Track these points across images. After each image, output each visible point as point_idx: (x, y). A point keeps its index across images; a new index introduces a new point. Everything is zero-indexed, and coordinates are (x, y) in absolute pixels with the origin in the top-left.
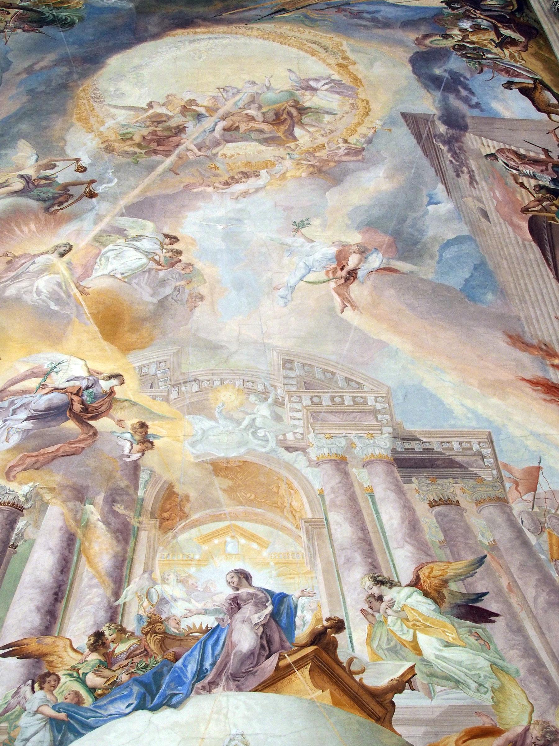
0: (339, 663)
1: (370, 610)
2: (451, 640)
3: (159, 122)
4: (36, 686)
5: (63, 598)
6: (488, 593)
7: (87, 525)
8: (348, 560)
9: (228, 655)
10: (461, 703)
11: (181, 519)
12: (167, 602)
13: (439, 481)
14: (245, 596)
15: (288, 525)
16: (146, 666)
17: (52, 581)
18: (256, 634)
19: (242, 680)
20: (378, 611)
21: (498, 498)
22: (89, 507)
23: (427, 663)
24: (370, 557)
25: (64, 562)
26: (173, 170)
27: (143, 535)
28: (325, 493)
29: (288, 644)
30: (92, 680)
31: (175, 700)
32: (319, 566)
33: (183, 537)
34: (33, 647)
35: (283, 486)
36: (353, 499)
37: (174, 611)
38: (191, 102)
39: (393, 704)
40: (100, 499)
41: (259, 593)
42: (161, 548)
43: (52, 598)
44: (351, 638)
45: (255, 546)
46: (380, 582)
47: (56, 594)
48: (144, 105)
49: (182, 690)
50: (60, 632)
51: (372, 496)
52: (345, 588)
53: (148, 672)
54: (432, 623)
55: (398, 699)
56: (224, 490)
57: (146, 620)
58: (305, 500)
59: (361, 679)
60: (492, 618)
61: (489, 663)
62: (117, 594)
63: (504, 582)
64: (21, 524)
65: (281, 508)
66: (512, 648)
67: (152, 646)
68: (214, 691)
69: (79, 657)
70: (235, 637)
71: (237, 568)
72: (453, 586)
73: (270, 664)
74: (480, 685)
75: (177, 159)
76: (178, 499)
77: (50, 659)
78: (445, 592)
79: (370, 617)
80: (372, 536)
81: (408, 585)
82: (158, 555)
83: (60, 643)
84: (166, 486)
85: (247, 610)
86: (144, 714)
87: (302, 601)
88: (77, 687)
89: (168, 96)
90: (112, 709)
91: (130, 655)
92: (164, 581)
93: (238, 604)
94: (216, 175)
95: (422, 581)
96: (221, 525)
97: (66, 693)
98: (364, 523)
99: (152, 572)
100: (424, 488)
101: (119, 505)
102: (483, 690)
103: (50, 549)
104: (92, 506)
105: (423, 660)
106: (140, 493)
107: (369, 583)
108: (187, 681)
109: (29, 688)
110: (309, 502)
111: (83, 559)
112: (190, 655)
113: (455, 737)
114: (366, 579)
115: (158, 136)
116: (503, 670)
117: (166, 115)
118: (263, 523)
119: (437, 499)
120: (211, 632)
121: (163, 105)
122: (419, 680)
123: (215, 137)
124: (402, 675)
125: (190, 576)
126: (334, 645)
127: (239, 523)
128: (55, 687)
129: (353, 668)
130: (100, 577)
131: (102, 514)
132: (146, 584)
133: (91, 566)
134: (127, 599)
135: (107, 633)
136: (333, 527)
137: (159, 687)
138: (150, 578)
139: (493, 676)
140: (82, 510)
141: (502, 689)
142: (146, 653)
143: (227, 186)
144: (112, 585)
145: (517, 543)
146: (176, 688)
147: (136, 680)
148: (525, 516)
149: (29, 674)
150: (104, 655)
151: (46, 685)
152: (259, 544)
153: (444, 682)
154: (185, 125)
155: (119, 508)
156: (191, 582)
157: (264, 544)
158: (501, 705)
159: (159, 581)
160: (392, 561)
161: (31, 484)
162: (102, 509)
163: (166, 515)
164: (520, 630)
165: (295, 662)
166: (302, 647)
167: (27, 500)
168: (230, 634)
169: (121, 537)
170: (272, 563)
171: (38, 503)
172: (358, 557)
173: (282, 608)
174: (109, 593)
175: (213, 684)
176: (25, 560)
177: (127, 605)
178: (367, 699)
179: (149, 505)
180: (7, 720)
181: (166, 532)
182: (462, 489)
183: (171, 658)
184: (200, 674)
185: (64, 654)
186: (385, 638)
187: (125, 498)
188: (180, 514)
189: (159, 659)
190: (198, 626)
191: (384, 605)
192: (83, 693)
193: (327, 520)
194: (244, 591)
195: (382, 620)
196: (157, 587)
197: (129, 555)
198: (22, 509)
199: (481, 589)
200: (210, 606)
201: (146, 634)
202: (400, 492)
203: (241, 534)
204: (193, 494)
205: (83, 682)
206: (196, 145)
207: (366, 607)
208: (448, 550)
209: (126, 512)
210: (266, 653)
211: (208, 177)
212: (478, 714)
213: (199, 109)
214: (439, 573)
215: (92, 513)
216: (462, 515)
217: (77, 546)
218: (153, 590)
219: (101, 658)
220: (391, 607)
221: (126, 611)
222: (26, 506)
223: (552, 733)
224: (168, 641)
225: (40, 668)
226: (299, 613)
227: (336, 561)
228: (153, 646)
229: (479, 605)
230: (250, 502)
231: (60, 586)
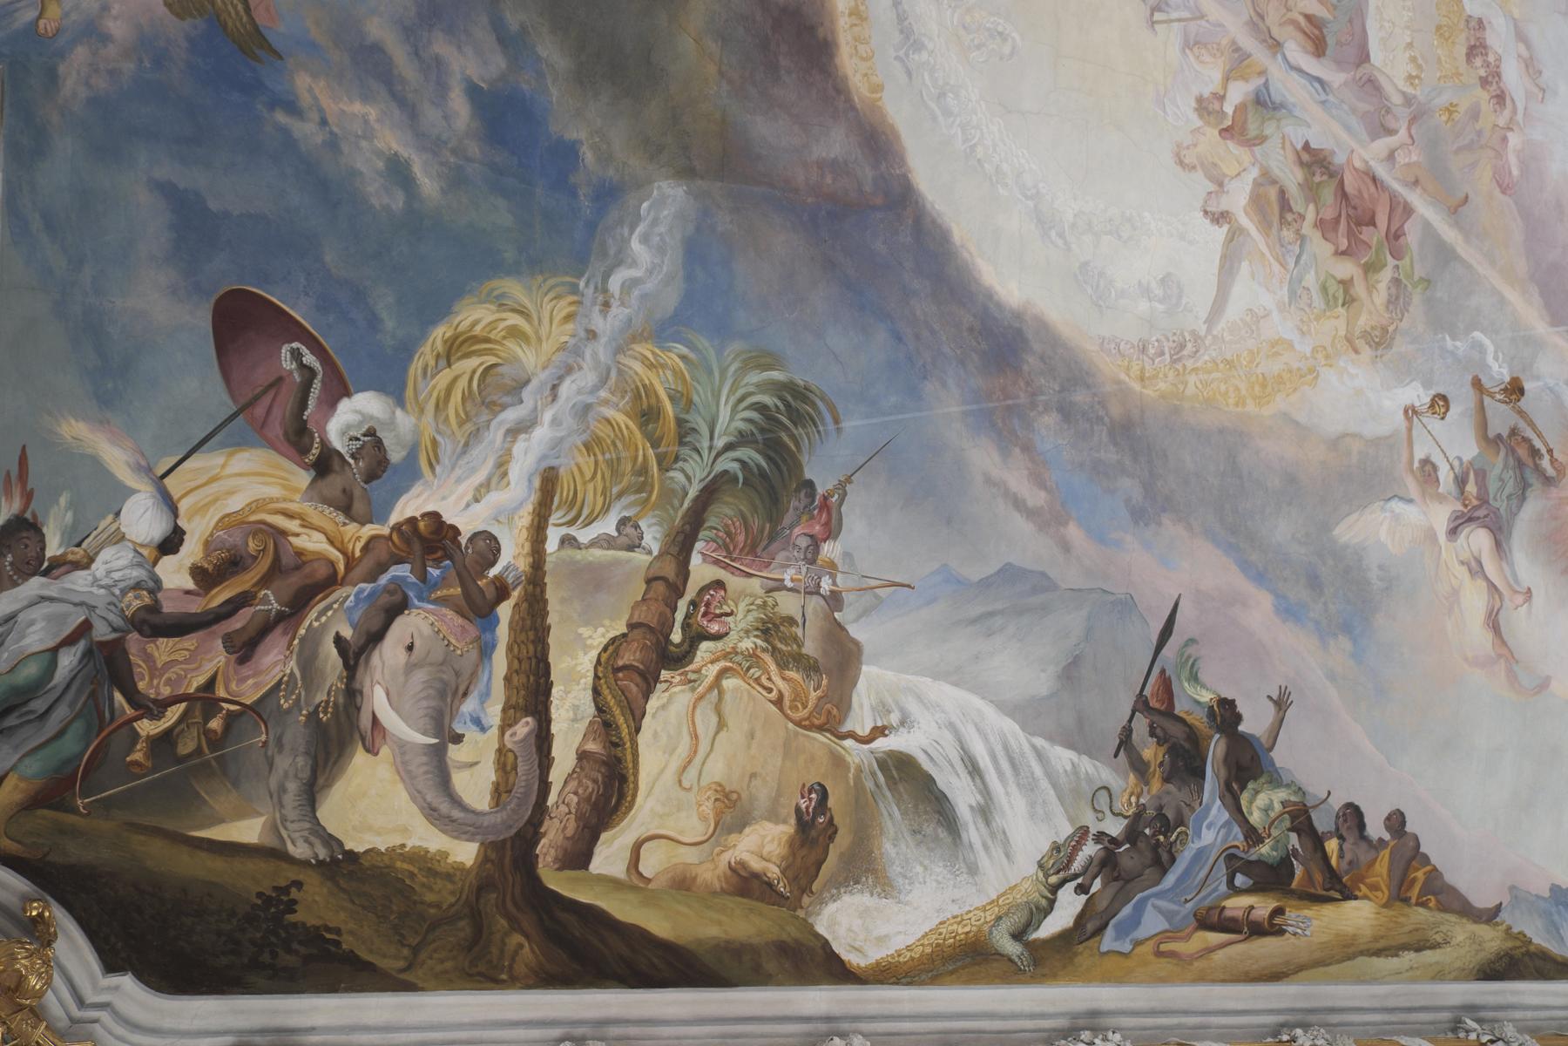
3: (1285, 204)
26: (1457, 208)
38: (1206, 107)
48: (1221, 232)
75: (1419, 190)
89: (1181, 163)
94: (1475, 114)
115: (1337, 220)
117: (1257, 184)
121: (1221, 185)
123: (1345, 84)
143: (1508, 101)
154: (1299, 146)
206: (1374, 136)
211: (1479, 133)
213: (1238, 93)
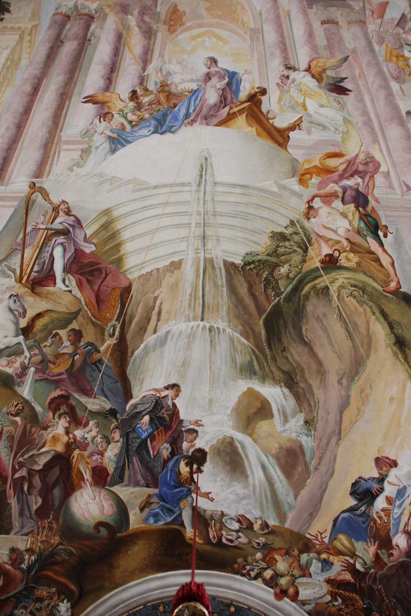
0: (262, 113)
1: (281, 84)
2: (324, 103)
4: (102, 119)
5: (115, 71)
6: (347, 78)
7: (128, 28)
8: (272, 54)
9: (202, 106)
10: (325, 138)
11: (181, 25)
12: (171, 75)
13: (329, 8)
14: (213, 72)
15: (240, 31)
16: (159, 110)
17: (109, 60)
18: (219, 94)
19: (209, 119)
20: (286, 85)
21: (361, 21)
22: (130, 17)
23: (309, 115)
24: (284, 53)
25: (116, 50)
27: (159, 35)
28: (263, 12)
29: (235, 101)
30: (130, 117)
31: (173, 129)
32: (256, 56)
33: (181, 37)
34: (100, 98)
35: (239, 7)
36: (278, 17)
37: (174, 80)
39: (289, 137)
40: (136, 12)
41: (221, 71)
42: (169, 43)
43: (110, 71)
44: (269, 99)
45: (221, 43)
46: (289, 68)
47: (112, 68)
49: (178, 124)
50: (114, 90)
51: (289, 16)
52: (269, 70)
53: (160, 113)
54: (315, 93)
55: (291, 134)
56: (206, 9)
57: (159, 84)
58: (251, 17)
59: (273, 122)
60: (347, 92)
61: (342, 118)
62: (144, 69)
63: (357, 72)
64: (93, 27)
65: (237, 21)
66: (356, 110)
67: (162, 99)
68: (194, 125)
69: (124, 104)
70: (207, 96)
71: (210, 56)
72: (329, 73)
74: (336, 129)
76: (179, 14)
77: (109, 104)
78: (324, 76)
79: (281, 88)
80: (287, 40)
81: (304, 71)
82: (167, 47)
83: (114, 96)
84: (173, 6)
86: (157, 136)
87: (244, 77)
88: (123, 120)
90: (140, 133)
92: (170, 62)
93: (210, 77)
95: (312, 69)
96: (203, 30)
97: (117, 124)
98: (283, 32)
99: (163, 56)
100: (319, 12)
101: (146, 16)
102: (337, 132)
103: (109, 42)
104: (131, 17)
105: (308, 114)
106: (158, 9)
107: (282, 68)
108: (180, 119)
109: (98, 120)
110: (253, 18)
111: (126, 48)
112: (182, 105)
113: (320, 156)
114: (281, 66)
116: (349, 122)
118: (226, 30)
119: (326, 20)
122: (304, 125)
124: (295, 121)
125: (184, 60)
126: (260, 102)
127: (213, 29)
128: (111, 120)
129: (269, 116)
130: (135, 59)
131: (137, 22)
132: (160, 64)
133: (131, 53)
134: (149, 72)
135: (138, 91)
136: (265, 34)
137: (165, 122)
138: (162, 60)
139: (344, 125)
140: (126, 19)
141: (347, 132)
142: (159, 103)
144: (142, 64)
145: (368, 49)
146: (174, 123)
147: (154, 118)
148: (374, 33)
149: (98, 112)
150: (137, 103)
151: (107, 119)
152: (224, 43)
153: (317, 127)
155: (147, 18)
156: (185, 63)
157: (226, 42)
158: (346, 141)
159: (167, 62)
160: (297, 56)
161: (98, 2)
162: (137, 18)
163: (172, 23)
164: (362, 100)
165: (238, 111)
166: (243, 103)
167: (96, 12)
168: (204, 94)
169: (147, 36)
170: (229, 54)
171: (102, 14)
172: (278, 52)
173: (233, 80)
175: (194, 121)
176: (95, 48)
177: (149, 76)
178: (275, 133)
179: (163, 17)
180: (88, 137)
181: (172, 33)
182: (341, 14)
183: (172, 106)
184: (187, 115)
185: (115, 102)
186: (288, 100)
187: (150, 12)
188: (180, 23)
189: (166, 106)
190: (187, 89)
191: (289, 81)
192: (126, 124)
193: (262, 29)
194: (213, 69)
195: (288, 89)
196: (166, 66)
197: (151, 46)
198: (93, 18)
199: (343, 76)
200: (194, 78)
201: (159, 92)
202: (305, 14)
203: (214, 36)
204: (188, 11)
205: (126, 118)
207: (279, 82)
208: (328, 51)
209: (150, 21)
210: (223, 105)
212: (333, 145)
214: (322, 64)
215: (131, 21)
216: (339, 31)
217: (123, 40)
218: (163, 67)
219: (135, 105)
220: (293, 83)
221: (149, 79)
222: (95, 16)
223: (369, 157)
224: (170, 97)
225: (104, 109)
226: (242, 83)
227: (265, 54)
228: (163, 99)
229: (341, 84)
230: (220, 17)
231: (114, 64)
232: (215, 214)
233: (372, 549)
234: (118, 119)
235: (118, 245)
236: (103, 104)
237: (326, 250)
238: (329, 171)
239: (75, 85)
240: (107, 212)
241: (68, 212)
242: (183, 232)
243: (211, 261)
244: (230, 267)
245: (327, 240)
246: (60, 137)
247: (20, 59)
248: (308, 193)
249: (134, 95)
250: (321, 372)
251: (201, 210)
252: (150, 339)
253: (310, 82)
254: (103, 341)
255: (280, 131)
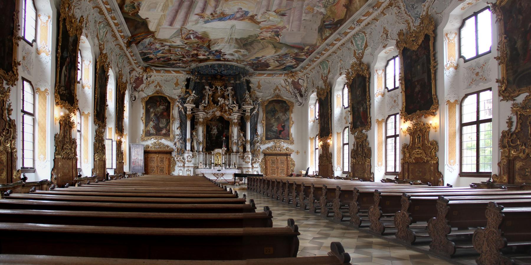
33: (229, 3)
34: (200, 14)
45: (245, 5)
46: (267, 11)
62: (215, 9)
73: (241, 18)
85: (239, 13)
86: (219, 22)
91: (217, 16)
111: (209, 4)
120: (232, 14)
126: (254, 17)
132: (221, 8)
142: (220, 16)
174: (214, 9)
176: (197, 4)
184: (229, 18)
194: (240, 10)
200: (233, 11)
232: (234, 32)
233: (257, 62)
234: (206, 19)
235: (208, 36)
236: (201, 15)
237: (262, 38)
238: (270, 28)
239: (191, 11)
240: (204, 31)
241: (193, 31)
242: (225, 34)
243: (232, 38)
244: (236, 39)
245: (263, 37)
246: (188, 20)
247: (168, 5)
248: (261, 31)
249: (212, 14)
250: (254, 49)
251: (231, 32)
252: (215, 45)
253: (274, 13)
254: (204, 44)
255: (258, 22)
